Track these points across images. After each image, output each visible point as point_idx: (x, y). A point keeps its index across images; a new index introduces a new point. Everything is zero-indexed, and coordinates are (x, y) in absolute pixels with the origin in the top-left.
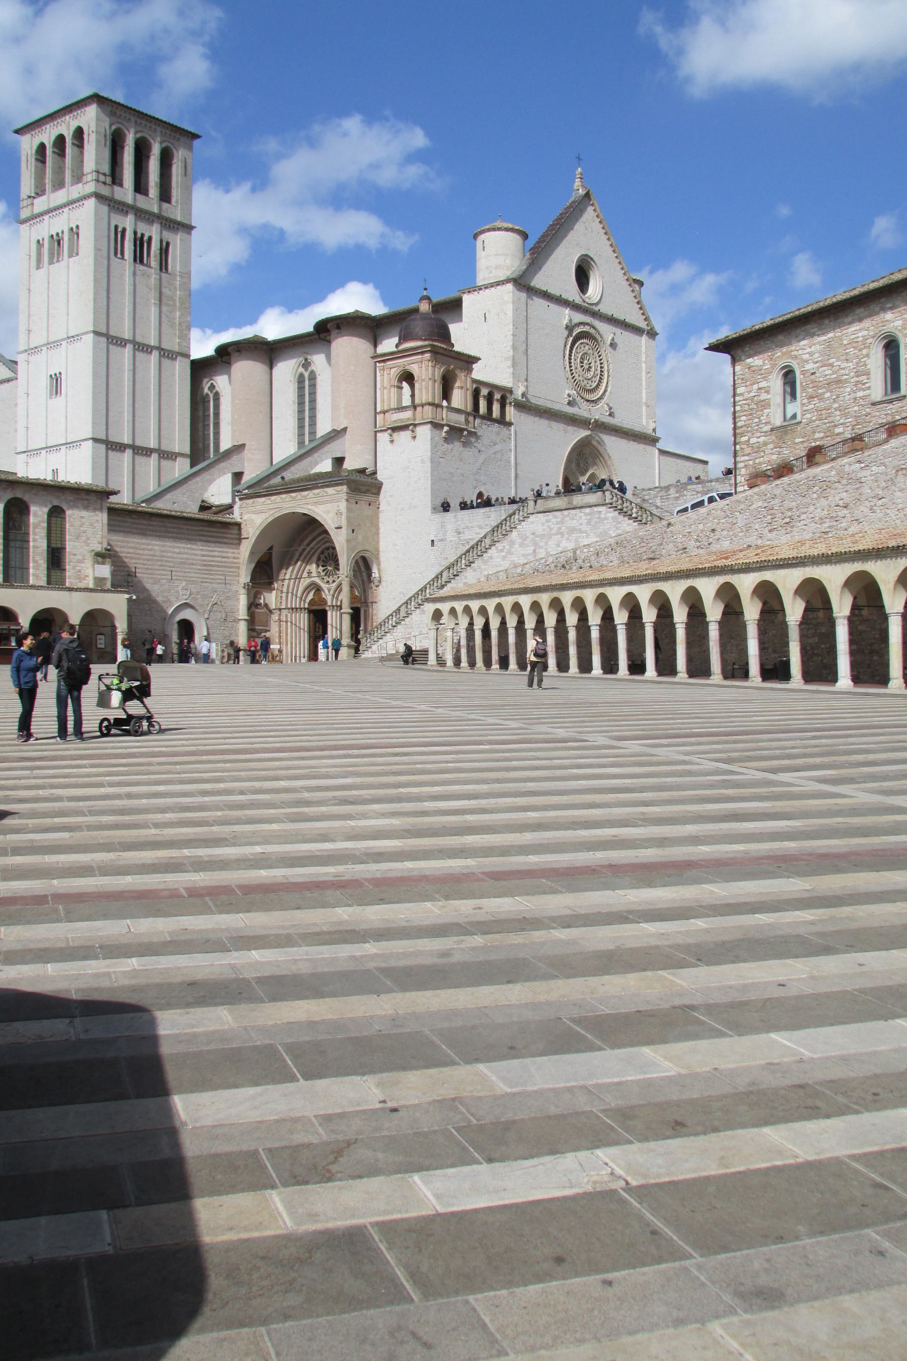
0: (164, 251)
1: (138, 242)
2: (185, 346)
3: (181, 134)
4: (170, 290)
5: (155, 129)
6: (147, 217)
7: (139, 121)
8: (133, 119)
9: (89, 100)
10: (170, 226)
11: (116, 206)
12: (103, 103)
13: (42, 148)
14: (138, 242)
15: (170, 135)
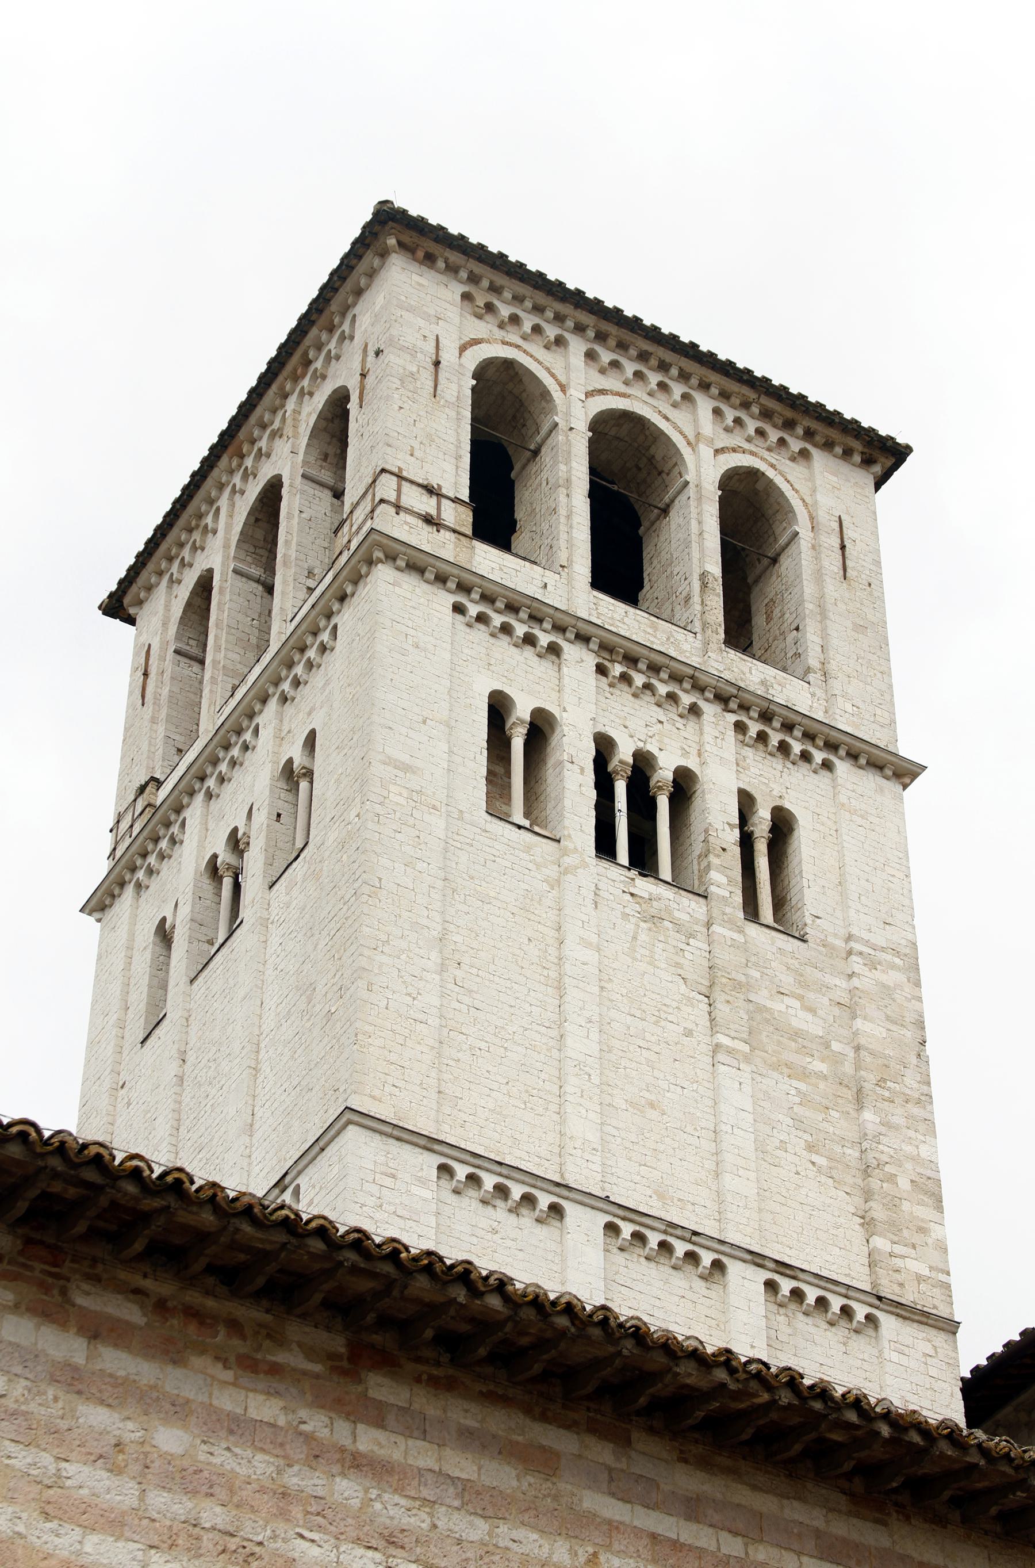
0: (761, 848)
1: (621, 788)
2: (920, 1278)
3: (809, 435)
4: (812, 1010)
5: (685, 397)
6: (663, 689)
7: (606, 356)
8: (577, 346)
9: (370, 259)
10: (784, 748)
11: (497, 620)
12: (429, 259)
13: (204, 587)
14: (621, 788)
15: (760, 433)
